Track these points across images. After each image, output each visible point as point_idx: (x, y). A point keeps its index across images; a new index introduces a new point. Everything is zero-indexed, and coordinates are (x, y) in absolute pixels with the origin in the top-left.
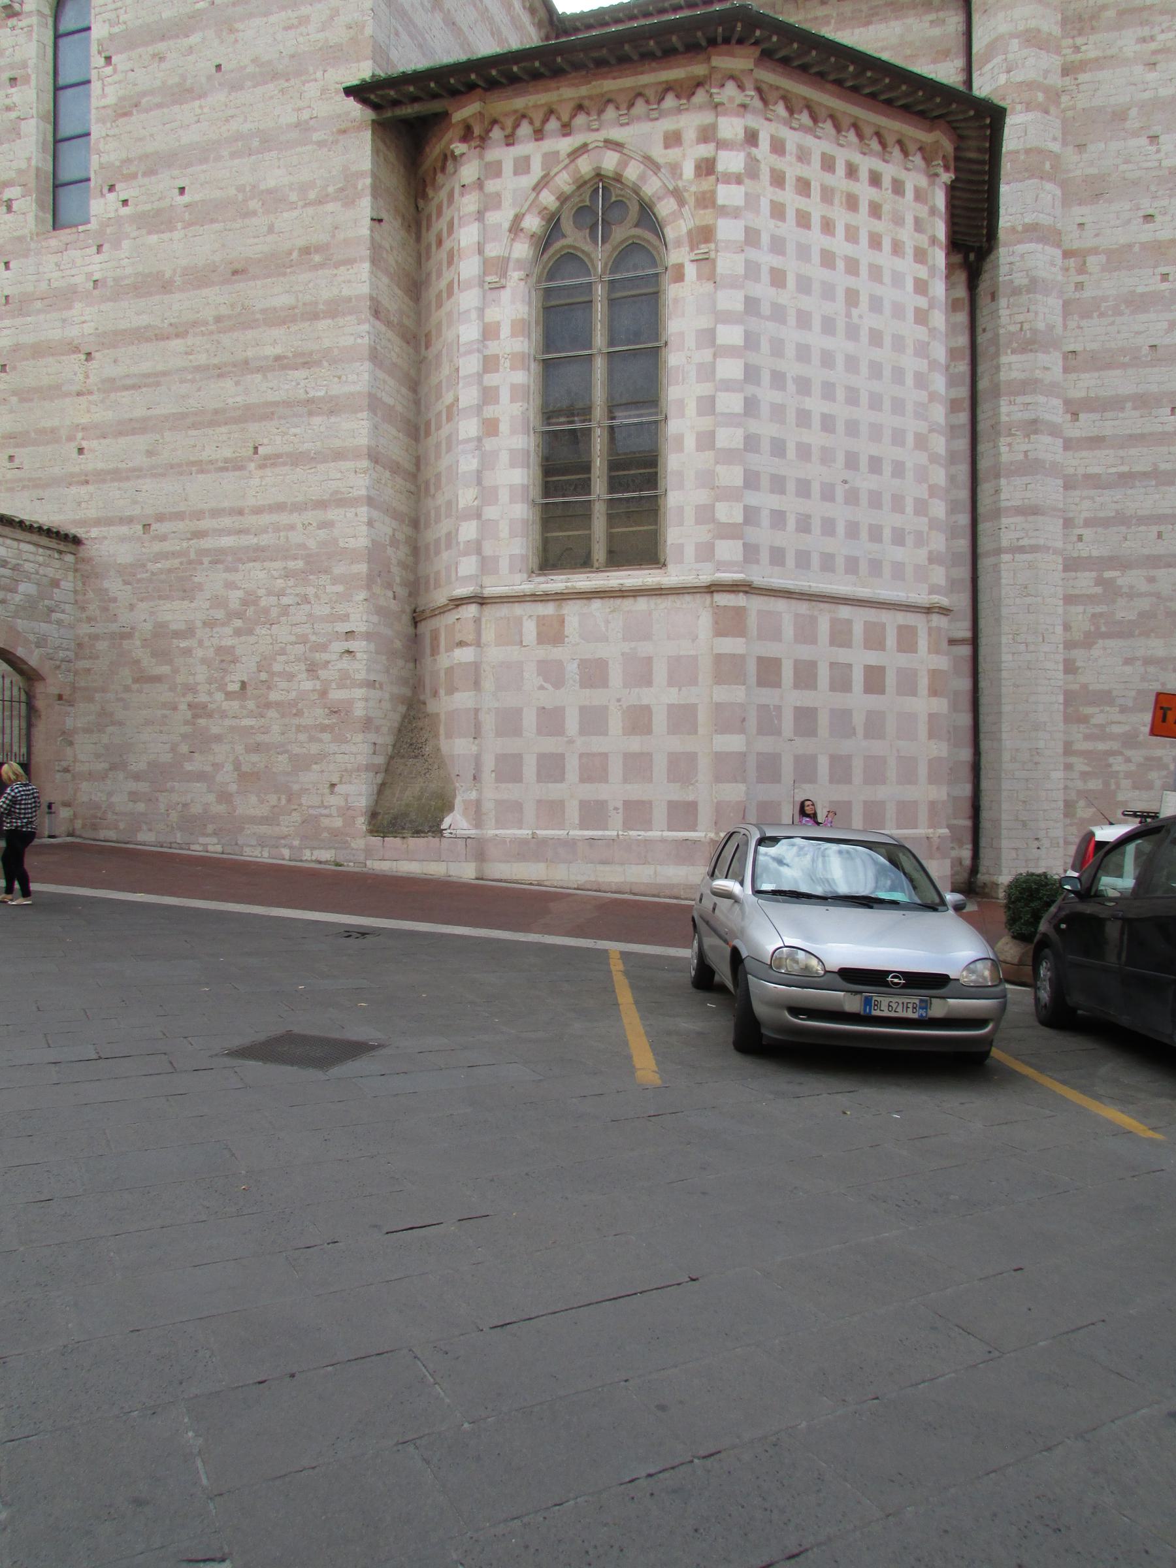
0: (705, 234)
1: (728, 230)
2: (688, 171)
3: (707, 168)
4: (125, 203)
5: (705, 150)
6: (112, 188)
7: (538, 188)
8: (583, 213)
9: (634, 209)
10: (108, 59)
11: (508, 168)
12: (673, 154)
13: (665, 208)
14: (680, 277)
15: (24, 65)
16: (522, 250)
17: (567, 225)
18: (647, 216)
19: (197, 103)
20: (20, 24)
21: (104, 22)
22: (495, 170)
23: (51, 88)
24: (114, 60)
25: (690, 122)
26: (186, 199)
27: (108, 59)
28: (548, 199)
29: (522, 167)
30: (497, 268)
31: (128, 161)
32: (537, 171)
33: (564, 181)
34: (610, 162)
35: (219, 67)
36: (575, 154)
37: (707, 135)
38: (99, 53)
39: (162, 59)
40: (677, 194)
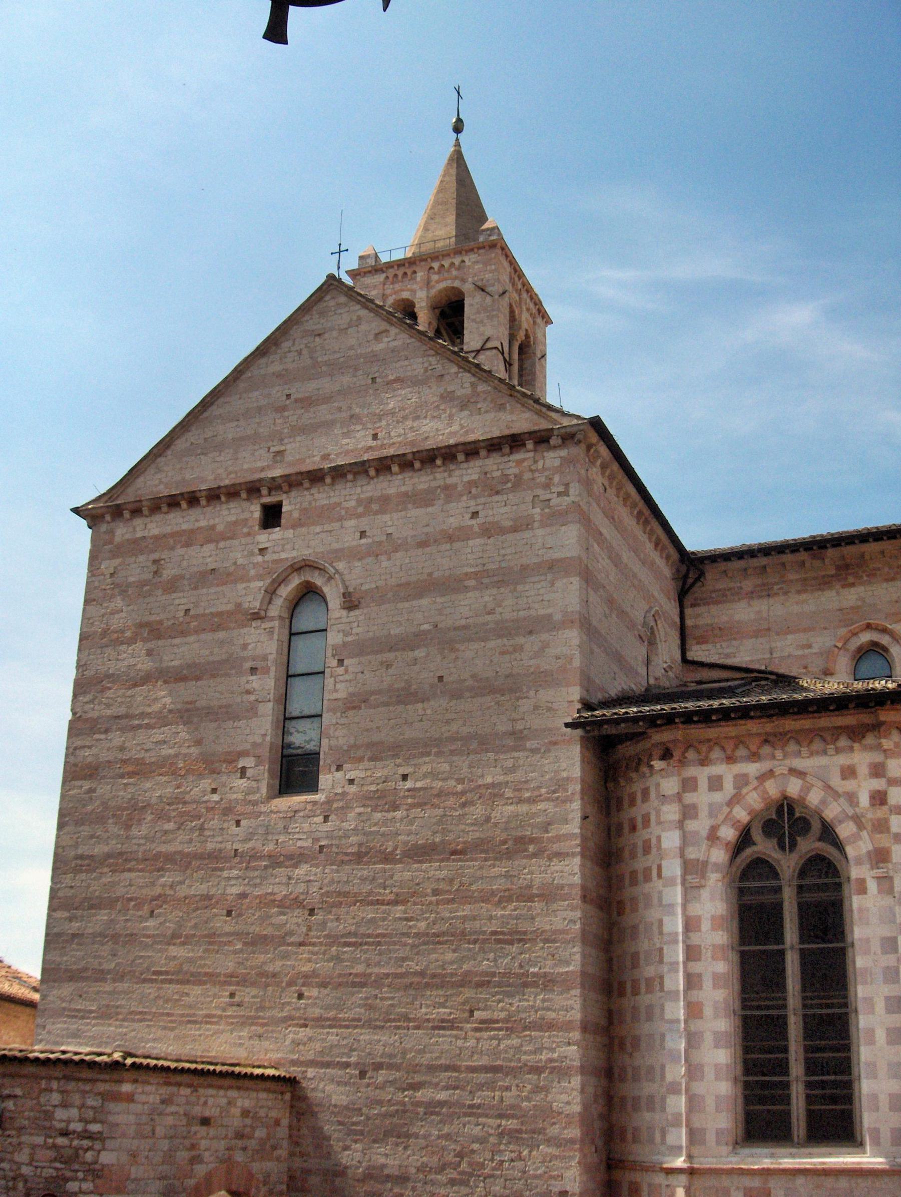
0: (880, 857)
2: (864, 800)
4: (351, 782)
5: (878, 784)
6: (339, 768)
7: (730, 803)
8: (771, 827)
9: (816, 826)
10: (341, 662)
11: (703, 784)
12: (849, 785)
13: (844, 831)
14: (863, 890)
15: (265, 658)
16: (719, 856)
17: (757, 835)
18: (828, 833)
19: (420, 705)
20: (263, 626)
21: (339, 632)
22: (689, 785)
23: (285, 676)
24: (346, 662)
26: (409, 784)
27: (341, 662)
28: (741, 815)
29: (715, 784)
31: (355, 747)
32: (729, 787)
33: (754, 799)
34: (794, 788)
35: (441, 678)
36: (762, 778)
37: (878, 771)
38: (333, 656)
39: (389, 666)
40: (857, 820)
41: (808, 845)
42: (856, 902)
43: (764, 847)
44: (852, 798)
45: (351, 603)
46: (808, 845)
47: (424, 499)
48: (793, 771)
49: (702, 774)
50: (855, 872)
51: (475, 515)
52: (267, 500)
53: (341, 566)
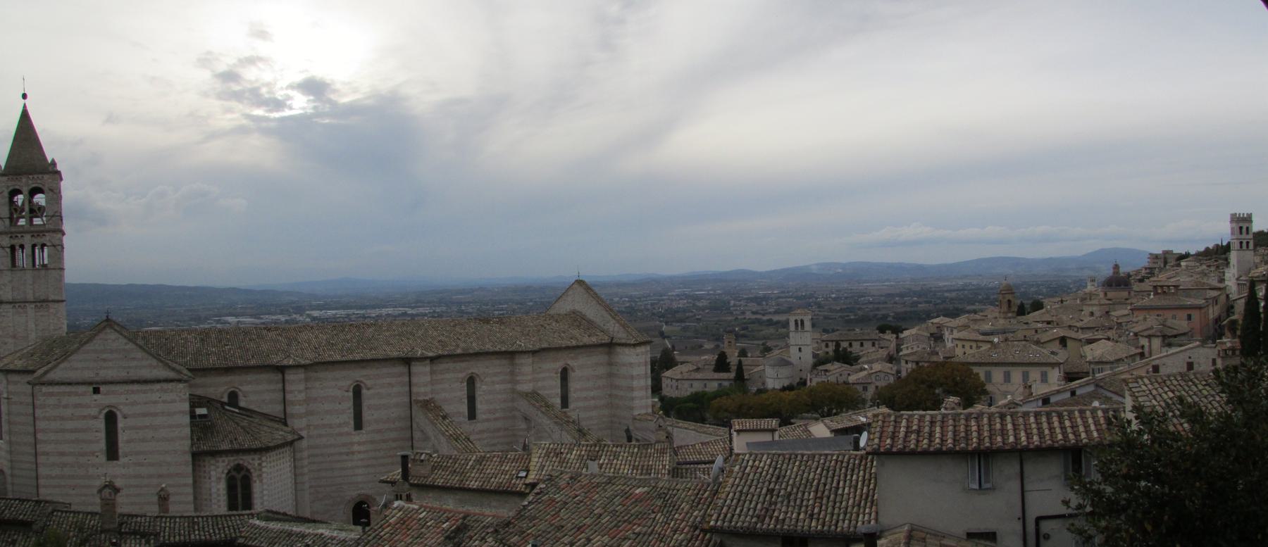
0: (260, 476)
1: (264, 475)
2: (256, 465)
3: (260, 464)
7: (227, 465)
8: (235, 469)
13: (252, 470)
14: (255, 482)
16: (224, 476)
18: (248, 470)
22: (218, 462)
25: (256, 457)
28: (229, 467)
29: (223, 461)
30: (219, 479)
33: (232, 464)
34: (241, 462)
40: (255, 469)
41: (243, 473)
42: (254, 485)
43: (234, 473)
44: (254, 465)
45: (125, 417)
46: (243, 473)
47: (145, 392)
48: (242, 459)
49: (220, 459)
50: (255, 479)
51: (160, 397)
52: (95, 386)
53: (122, 407)
